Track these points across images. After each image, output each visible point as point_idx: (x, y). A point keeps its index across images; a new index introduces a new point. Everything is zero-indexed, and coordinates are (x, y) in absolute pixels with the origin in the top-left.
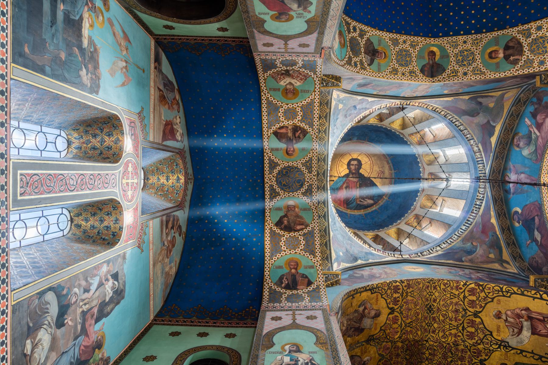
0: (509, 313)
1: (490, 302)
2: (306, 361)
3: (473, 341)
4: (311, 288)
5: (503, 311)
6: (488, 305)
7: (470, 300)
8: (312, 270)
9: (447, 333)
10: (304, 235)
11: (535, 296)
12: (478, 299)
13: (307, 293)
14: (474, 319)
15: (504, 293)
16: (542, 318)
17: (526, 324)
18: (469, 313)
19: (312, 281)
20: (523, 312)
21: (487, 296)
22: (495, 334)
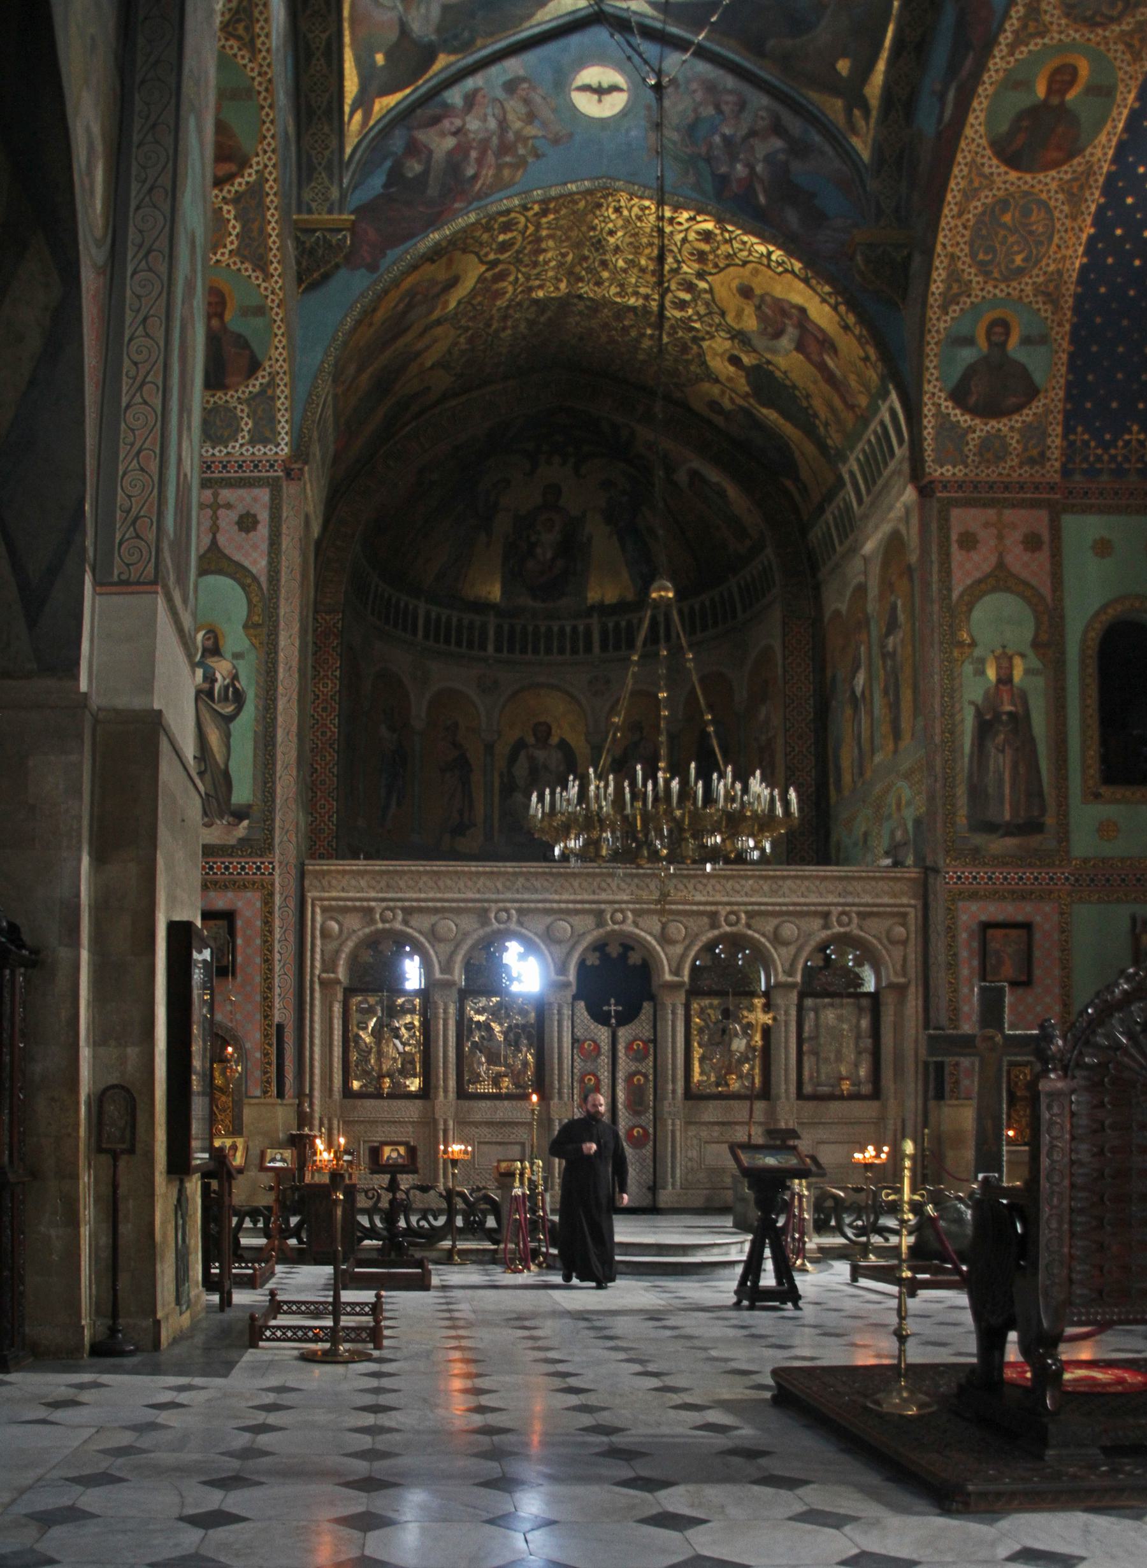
0: (768, 299)
1: (737, 265)
2: (227, 681)
3: (683, 314)
4: (255, 385)
5: (758, 292)
6: (732, 269)
7: (695, 249)
8: (259, 322)
9: (630, 290)
10: (237, 199)
11: (827, 297)
12: (713, 251)
13: (248, 402)
14: (696, 281)
15: (773, 264)
16: (821, 338)
17: (791, 332)
18: (685, 268)
19: (260, 357)
20: (793, 311)
21: (735, 254)
22: (730, 319)
